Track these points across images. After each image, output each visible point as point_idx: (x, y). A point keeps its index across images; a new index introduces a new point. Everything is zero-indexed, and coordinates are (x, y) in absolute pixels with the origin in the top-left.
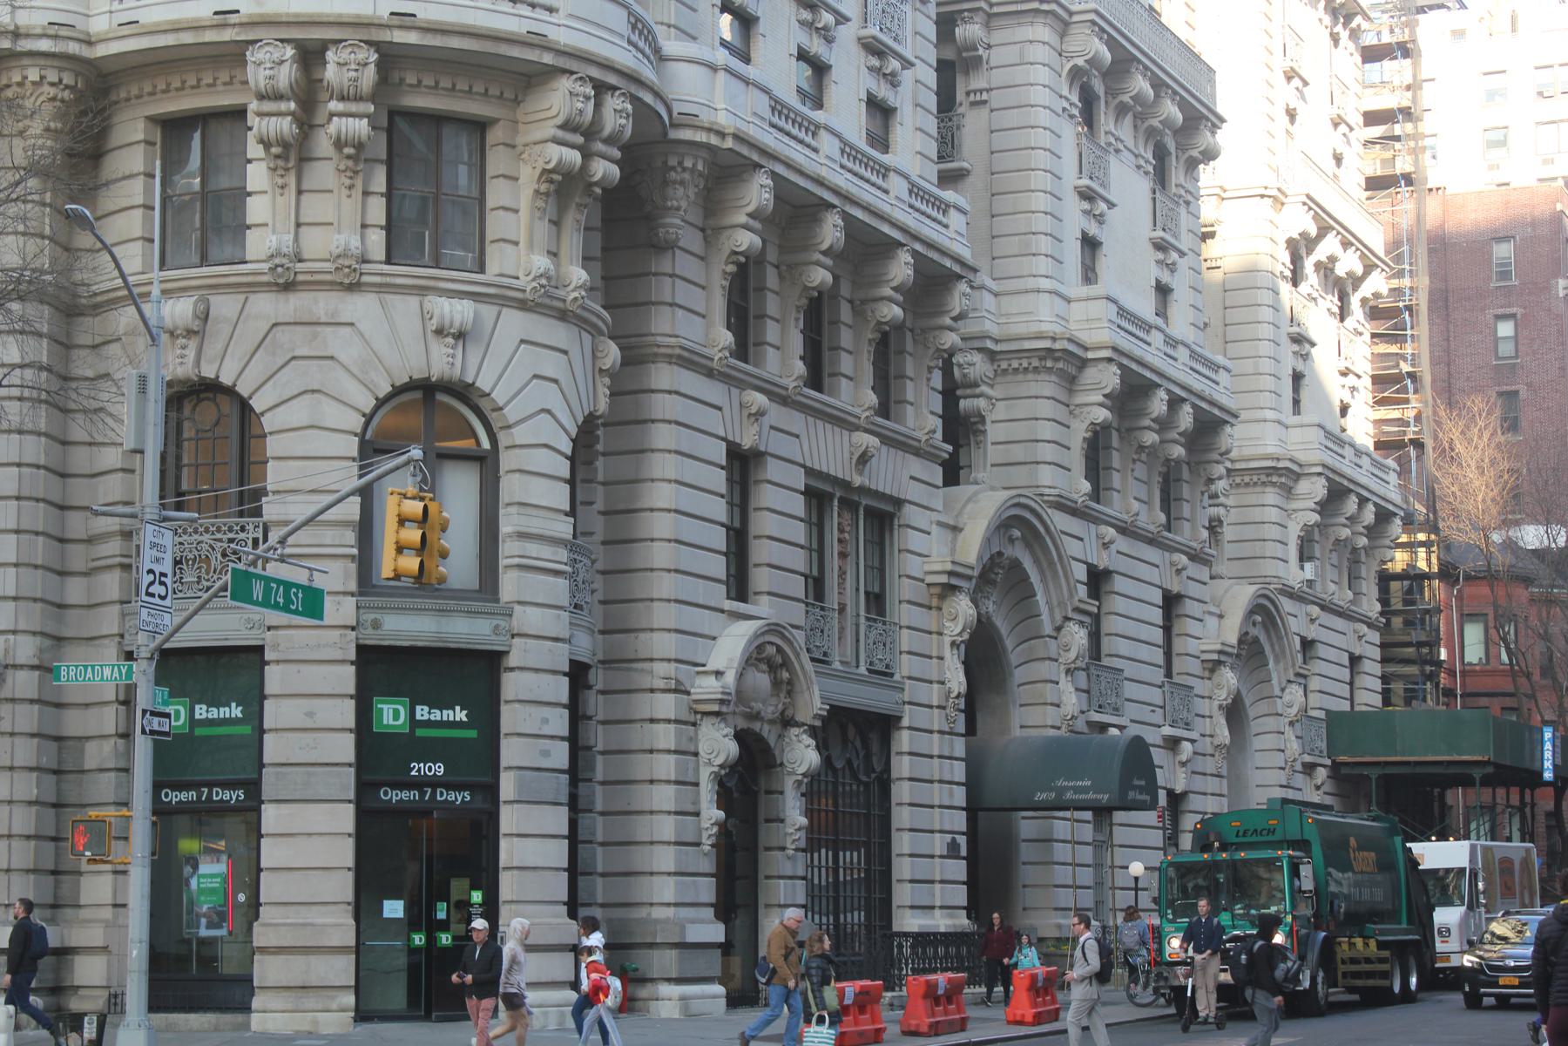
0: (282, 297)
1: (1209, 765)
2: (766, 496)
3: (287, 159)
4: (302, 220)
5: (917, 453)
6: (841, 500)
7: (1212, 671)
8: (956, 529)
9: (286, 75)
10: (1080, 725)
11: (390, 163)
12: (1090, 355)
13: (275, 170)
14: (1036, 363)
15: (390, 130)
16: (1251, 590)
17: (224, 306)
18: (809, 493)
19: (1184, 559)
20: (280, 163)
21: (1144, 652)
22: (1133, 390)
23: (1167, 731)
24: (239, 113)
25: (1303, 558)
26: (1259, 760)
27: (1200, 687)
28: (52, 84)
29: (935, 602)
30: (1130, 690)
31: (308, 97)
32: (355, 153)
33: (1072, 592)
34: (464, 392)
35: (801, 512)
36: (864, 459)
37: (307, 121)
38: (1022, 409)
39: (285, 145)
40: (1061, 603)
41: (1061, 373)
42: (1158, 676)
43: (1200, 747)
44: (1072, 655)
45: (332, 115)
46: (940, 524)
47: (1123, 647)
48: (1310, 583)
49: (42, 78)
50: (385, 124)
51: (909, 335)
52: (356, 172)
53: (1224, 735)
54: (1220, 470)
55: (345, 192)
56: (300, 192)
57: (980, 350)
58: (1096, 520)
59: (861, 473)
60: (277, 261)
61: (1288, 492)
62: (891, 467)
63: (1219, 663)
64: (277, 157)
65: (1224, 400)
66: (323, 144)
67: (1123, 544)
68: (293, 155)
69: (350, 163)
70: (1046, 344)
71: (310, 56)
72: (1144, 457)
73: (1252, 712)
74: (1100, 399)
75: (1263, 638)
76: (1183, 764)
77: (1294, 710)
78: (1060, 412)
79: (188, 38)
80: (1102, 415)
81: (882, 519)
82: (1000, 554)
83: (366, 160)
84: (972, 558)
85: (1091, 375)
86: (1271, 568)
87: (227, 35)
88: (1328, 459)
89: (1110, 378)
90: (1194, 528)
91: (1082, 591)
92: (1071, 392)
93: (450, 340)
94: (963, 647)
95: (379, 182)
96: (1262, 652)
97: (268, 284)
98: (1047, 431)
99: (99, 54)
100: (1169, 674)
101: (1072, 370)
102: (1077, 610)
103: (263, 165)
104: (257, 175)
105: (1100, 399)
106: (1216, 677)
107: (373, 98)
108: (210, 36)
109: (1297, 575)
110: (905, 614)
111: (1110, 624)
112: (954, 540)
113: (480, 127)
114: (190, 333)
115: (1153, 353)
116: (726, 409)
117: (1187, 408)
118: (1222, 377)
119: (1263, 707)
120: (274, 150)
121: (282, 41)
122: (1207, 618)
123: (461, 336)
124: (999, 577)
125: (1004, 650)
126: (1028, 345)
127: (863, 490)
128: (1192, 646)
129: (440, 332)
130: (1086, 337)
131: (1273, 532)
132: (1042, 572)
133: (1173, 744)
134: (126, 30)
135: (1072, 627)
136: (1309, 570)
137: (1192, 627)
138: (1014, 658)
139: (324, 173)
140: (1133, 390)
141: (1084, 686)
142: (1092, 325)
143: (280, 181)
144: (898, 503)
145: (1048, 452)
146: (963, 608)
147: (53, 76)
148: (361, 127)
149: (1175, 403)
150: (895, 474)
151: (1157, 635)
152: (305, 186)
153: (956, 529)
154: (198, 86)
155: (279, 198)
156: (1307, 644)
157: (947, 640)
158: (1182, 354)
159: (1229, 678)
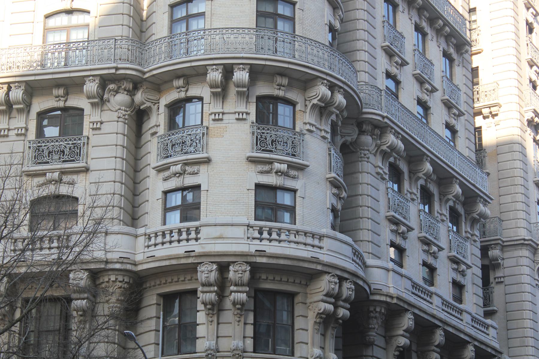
4: (219, 335)
9: (213, 276)
11: (255, 311)
13: (208, 315)
15: (255, 298)
20: (211, 312)
24: (194, 292)
28: (120, 282)
31: (222, 285)
32: (241, 307)
37: (221, 294)
39: (213, 304)
45: (232, 292)
49: (116, 279)
50: (253, 295)
52: (241, 315)
55: (237, 323)
56: (218, 324)
60: (209, 352)
64: (209, 309)
66: (228, 304)
68: (216, 309)
69: (239, 311)
71: (223, 268)
79: (174, 262)
83: (245, 310)
87: (190, 261)
95: (251, 318)
99: (139, 269)
103: (204, 313)
104: (201, 317)
107: (248, 284)
108: (183, 261)
113: (291, 296)
120: (208, 307)
121: (212, 262)
134: (150, 260)
139: (228, 315)
143: (210, 319)
147: (120, 278)
148: (243, 297)
152: (220, 321)
154: (178, 281)
155: (210, 326)
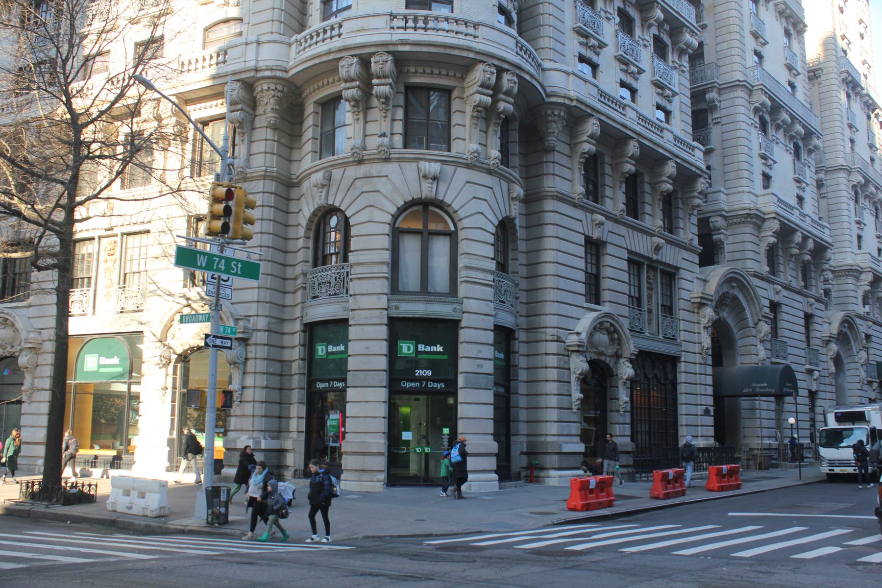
0: (358, 167)
1: (827, 381)
2: (607, 260)
3: (358, 107)
5: (686, 249)
6: (648, 265)
7: (827, 344)
8: (705, 281)
10: (768, 362)
12: (766, 217)
14: (743, 220)
16: (843, 314)
17: (337, 174)
18: (630, 261)
19: (813, 300)
21: (796, 336)
22: (786, 232)
23: (808, 367)
25: (864, 304)
26: (849, 379)
27: (821, 350)
29: (696, 310)
30: (790, 350)
33: (761, 309)
34: (441, 205)
35: (626, 269)
36: (658, 249)
38: (738, 238)
40: (757, 314)
41: (755, 224)
42: (804, 345)
43: (822, 373)
44: (762, 335)
46: (697, 278)
47: (787, 333)
48: (868, 313)
51: (680, 201)
52: (387, 110)
53: (833, 369)
54: (826, 266)
56: (366, 122)
57: (720, 215)
58: (773, 283)
59: (657, 254)
61: (857, 278)
62: (672, 254)
63: (829, 341)
65: (829, 240)
67: (784, 292)
70: (747, 212)
71: (365, 62)
72: (793, 259)
73: (845, 361)
74: (771, 233)
75: (849, 333)
76: (815, 380)
77: (862, 361)
78: (755, 240)
80: (773, 240)
81: (670, 275)
82: (727, 293)
84: (712, 292)
85: (767, 225)
86: (851, 307)
88: (873, 266)
89: (775, 225)
90: (817, 289)
91: (767, 310)
92: (759, 232)
93: (430, 181)
94: (710, 329)
96: (848, 338)
97: (352, 162)
98: (749, 246)
100: (809, 345)
101: (759, 223)
102: (763, 316)
105: (771, 233)
106: (829, 347)
109: (862, 310)
110: (682, 315)
111: (781, 324)
112: (705, 286)
114: (323, 186)
115: (795, 217)
116: (584, 222)
117: (811, 240)
118: (827, 231)
119: (850, 359)
122: (825, 324)
123: (435, 178)
124: (724, 301)
125: (733, 333)
126: (739, 213)
127: (657, 261)
128: (818, 334)
129: (425, 177)
130: (765, 210)
131: (852, 294)
132: (747, 301)
133: (810, 372)
135: (762, 324)
136: (867, 308)
137: (817, 327)
138: (737, 337)
140: (786, 232)
141: (769, 347)
142: (766, 204)
144: (677, 269)
145: (749, 255)
146: (709, 312)
149: (805, 238)
150: (670, 256)
151: (803, 330)
153: (705, 281)
156: (868, 337)
157: (702, 326)
158: (808, 220)
159: (834, 347)
